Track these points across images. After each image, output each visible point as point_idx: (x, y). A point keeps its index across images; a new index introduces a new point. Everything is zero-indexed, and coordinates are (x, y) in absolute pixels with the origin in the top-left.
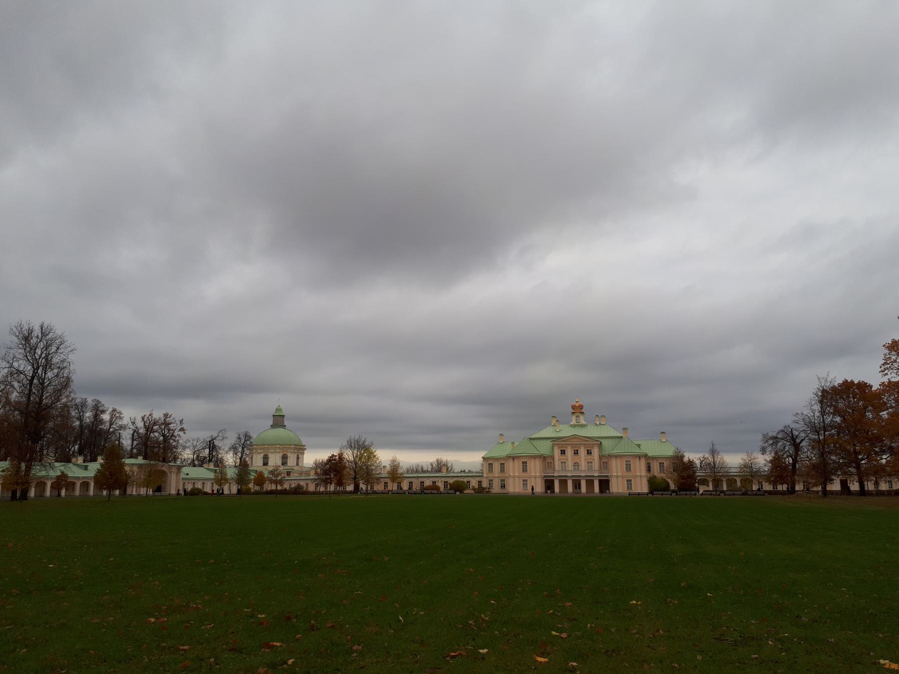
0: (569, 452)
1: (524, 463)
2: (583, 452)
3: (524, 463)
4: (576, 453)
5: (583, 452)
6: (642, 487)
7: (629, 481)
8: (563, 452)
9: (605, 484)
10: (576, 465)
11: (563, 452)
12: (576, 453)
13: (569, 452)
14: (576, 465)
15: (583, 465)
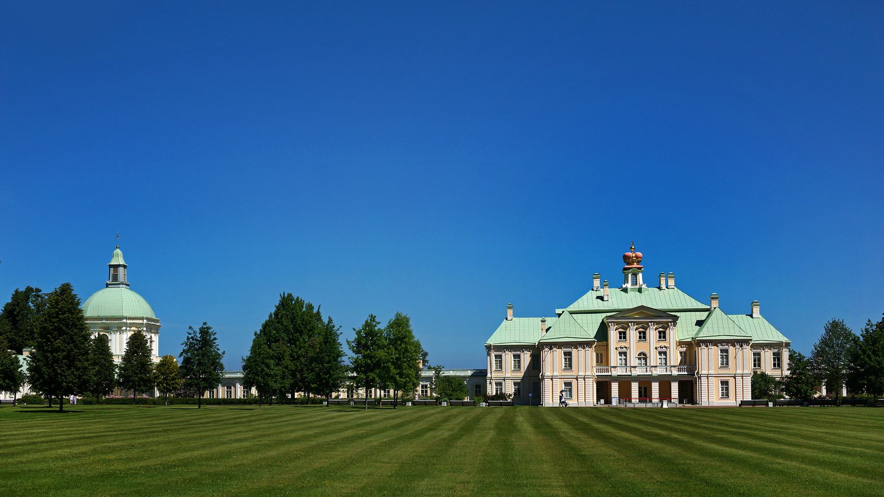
0: (633, 334)
1: (568, 355)
2: (653, 334)
3: (568, 355)
4: (643, 336)
5: (653, 334)
6: (743, 392)
7: (725, 383)
8: (623, 336)
9: (689, 389)
10: (643, 356)
11: (623, 336)
12: (643, 336)
13: (633, 334)
14: (643, 356)
15: (654, 358)
